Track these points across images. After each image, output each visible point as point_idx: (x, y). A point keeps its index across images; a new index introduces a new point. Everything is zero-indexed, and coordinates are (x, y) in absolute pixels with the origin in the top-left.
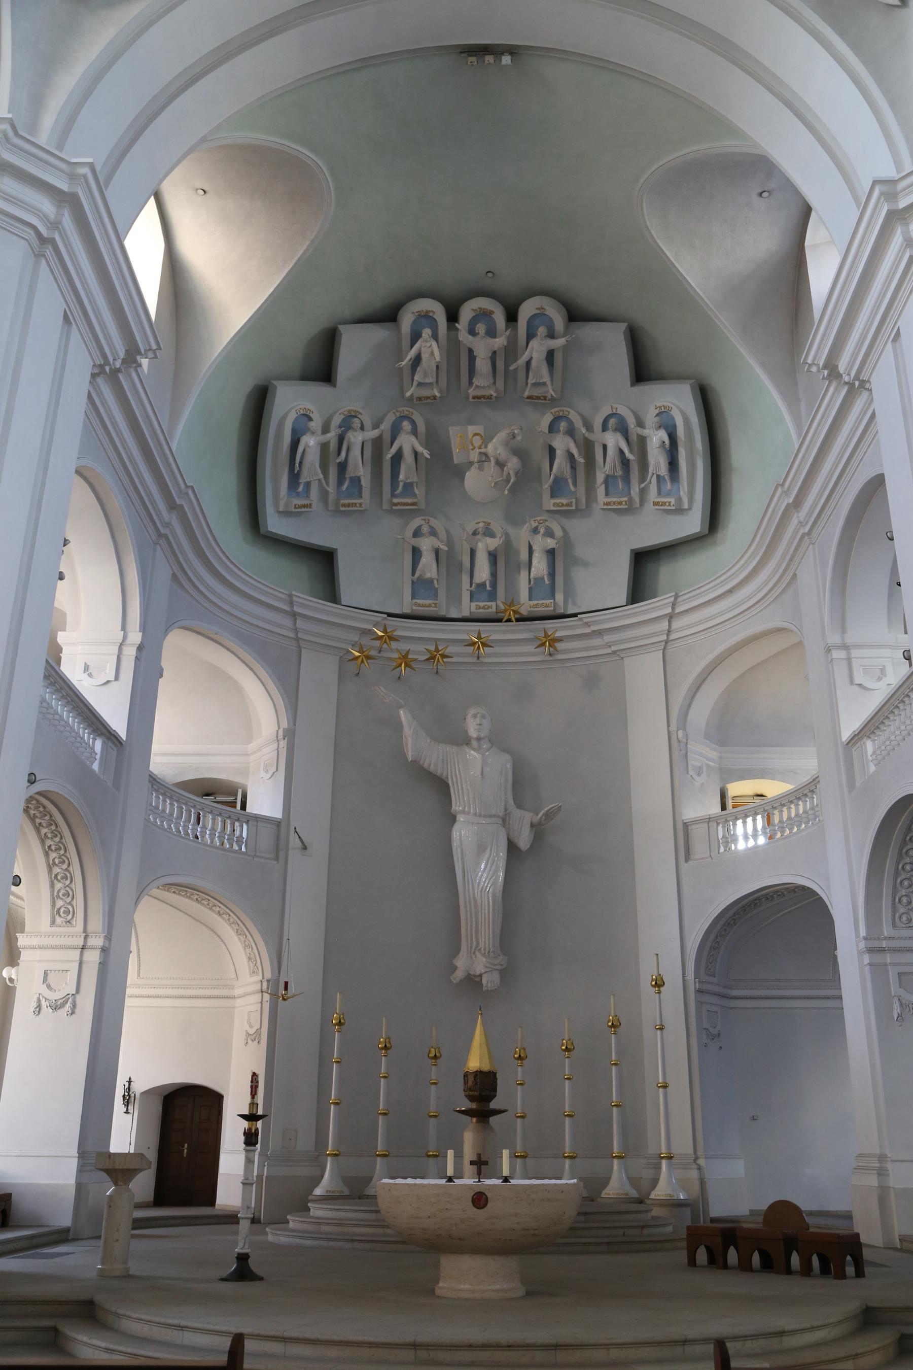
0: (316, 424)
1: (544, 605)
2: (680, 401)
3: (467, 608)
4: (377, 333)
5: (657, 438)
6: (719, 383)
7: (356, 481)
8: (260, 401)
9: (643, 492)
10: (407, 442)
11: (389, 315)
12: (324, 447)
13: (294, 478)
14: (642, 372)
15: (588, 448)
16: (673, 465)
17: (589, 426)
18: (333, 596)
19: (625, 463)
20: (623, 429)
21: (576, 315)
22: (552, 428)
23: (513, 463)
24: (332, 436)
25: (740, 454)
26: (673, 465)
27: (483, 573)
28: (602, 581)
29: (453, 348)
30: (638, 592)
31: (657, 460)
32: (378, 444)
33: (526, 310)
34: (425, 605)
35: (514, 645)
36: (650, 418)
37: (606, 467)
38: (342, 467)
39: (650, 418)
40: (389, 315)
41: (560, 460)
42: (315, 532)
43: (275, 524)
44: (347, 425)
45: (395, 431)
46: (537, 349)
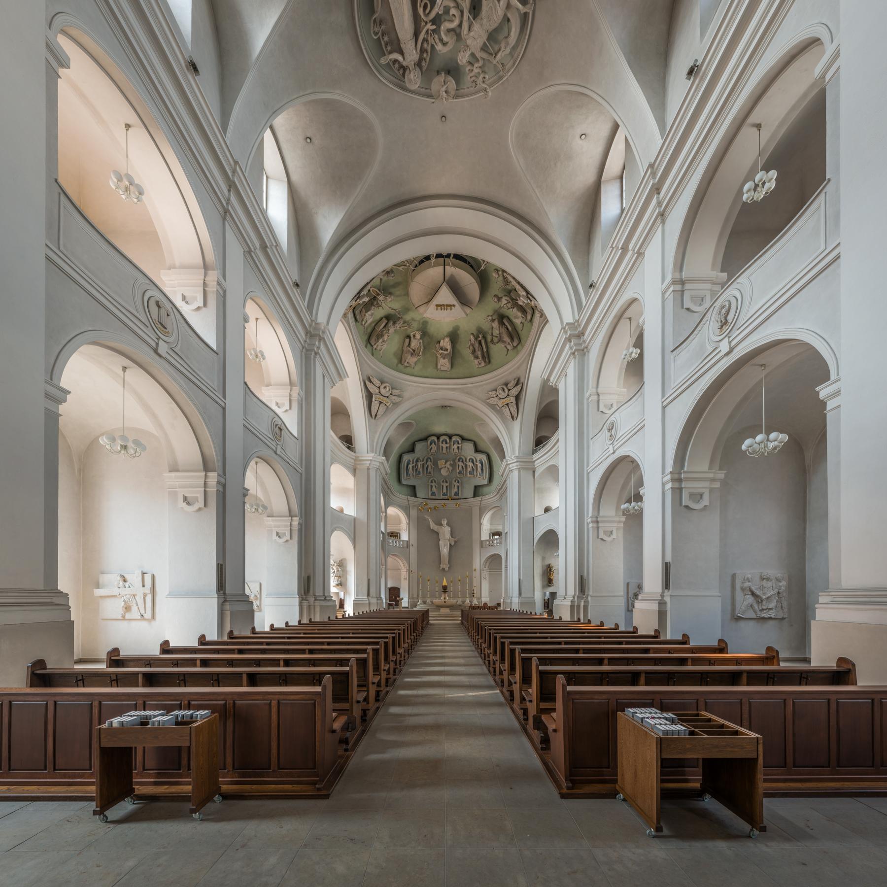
1: (457, 497)
2: (484, 458)
3: (442, 497)
4: (423, 443)
5: (479, 465)
6: (491, 455)
10: (429, 463)
11: (425, 439)
13: (407, 473)
14: (477, 450)
15: (466, 466)
16: (482, 470)
18: (415, 496)
20: (473, 462)
21: (463, 439)
23: (451, 468)
25: (495, 469)
26: (482, 470)
27: (445, 490)
28: (468, 491)
29: (438, 446)
30: (475, 495)
31: (479, 470)
33: (454, 439)
34: (433, 497)
35: (451, 504)
37: (469, 469)
40: (425, 439)
42: (411, 482)
43: (404, 482)
44: (417, 461)
46: (455, 446)
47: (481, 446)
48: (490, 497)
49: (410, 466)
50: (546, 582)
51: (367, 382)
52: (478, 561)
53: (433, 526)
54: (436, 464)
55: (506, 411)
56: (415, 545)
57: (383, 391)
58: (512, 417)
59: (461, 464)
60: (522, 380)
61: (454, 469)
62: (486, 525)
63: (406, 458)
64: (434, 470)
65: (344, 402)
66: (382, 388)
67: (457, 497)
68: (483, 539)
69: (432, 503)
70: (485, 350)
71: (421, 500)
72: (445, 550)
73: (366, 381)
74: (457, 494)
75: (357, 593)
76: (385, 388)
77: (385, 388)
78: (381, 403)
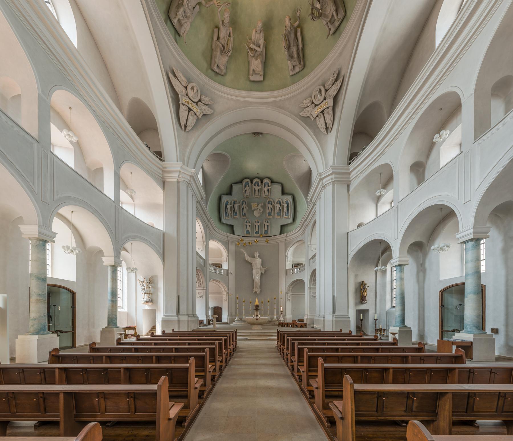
0: (229, 203)
2: (289, 198)
6: (296, 196)
7: (236, 213)
8: (220, 198)
9: (283, 215)
10: (244, 206)
12: (231, 207)
13: (226, 213)
15: (274, 207)
16: (288, 210)
17: (274, 203)
19: (280, 210)
22: (268, 203)
23: (262, 210)
24: (232, 205)
26: (288, 210)
32: (240, 206)
36: (284, 202)
37: (277, 211)
38: (234, 211)
39: (284, 202)
41: (270, 208)
44: (234, 203)
45: (242, 204)
47: (287, 189)
48: (294, 233)
49: (229, 206)
50: (359, 300)
51: (171, 76)
52: (283, 286)
53: (247, 258)
54: (250, 206)
56: (233, 273)
57: (191, 93)
58: (327, 128)
59: (270, 206)
60: (343, 73)
61: (264, 212)
62: (290, 257)
63: (225, 199)
64: (248, 200)
65: (149, 106)
67: (266, 235)
68: (287, 268)
69: (247, 240)
70: (300, 46)
71: (238, 237)
72: (257, 278)
73: (170, 74)
74: (266, 232)
75: (167, 310)
76: (192, 88)
77: (192, 88)
78: (190, 110)
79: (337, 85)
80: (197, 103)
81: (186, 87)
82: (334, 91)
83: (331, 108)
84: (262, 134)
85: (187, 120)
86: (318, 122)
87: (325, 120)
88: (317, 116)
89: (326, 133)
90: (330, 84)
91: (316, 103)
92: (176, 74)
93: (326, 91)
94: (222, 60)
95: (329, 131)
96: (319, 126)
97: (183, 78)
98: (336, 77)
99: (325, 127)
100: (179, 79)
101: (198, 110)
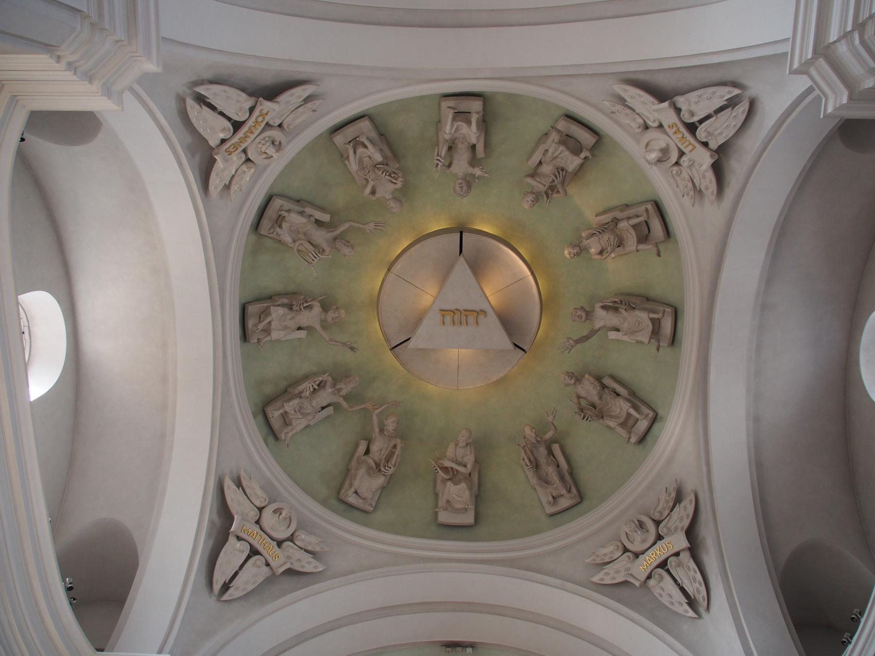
55: (665, 590)
58: (692, 603)
60: (689, 486)
66: (267, 514)
79: (685, 508)
80: (280, 544)
81: (261, 509)
82: (681, 519)
83: (685, 556)
84: (472, 645)
85: (236, 574)
86: (657, 591)
87: (679, 585)
88: (649, 577)
89: (691, 613)
90: (664, 508)
91: (636, 547)
92: (244, 483)
93: (657, 523)
94: (367, 484)
95: (702, 610)
96: (665, 600)
97: (260, 492)
98: (673, 495)
99: (684, 600)
100: (247, 491)
101: (281, 555)
